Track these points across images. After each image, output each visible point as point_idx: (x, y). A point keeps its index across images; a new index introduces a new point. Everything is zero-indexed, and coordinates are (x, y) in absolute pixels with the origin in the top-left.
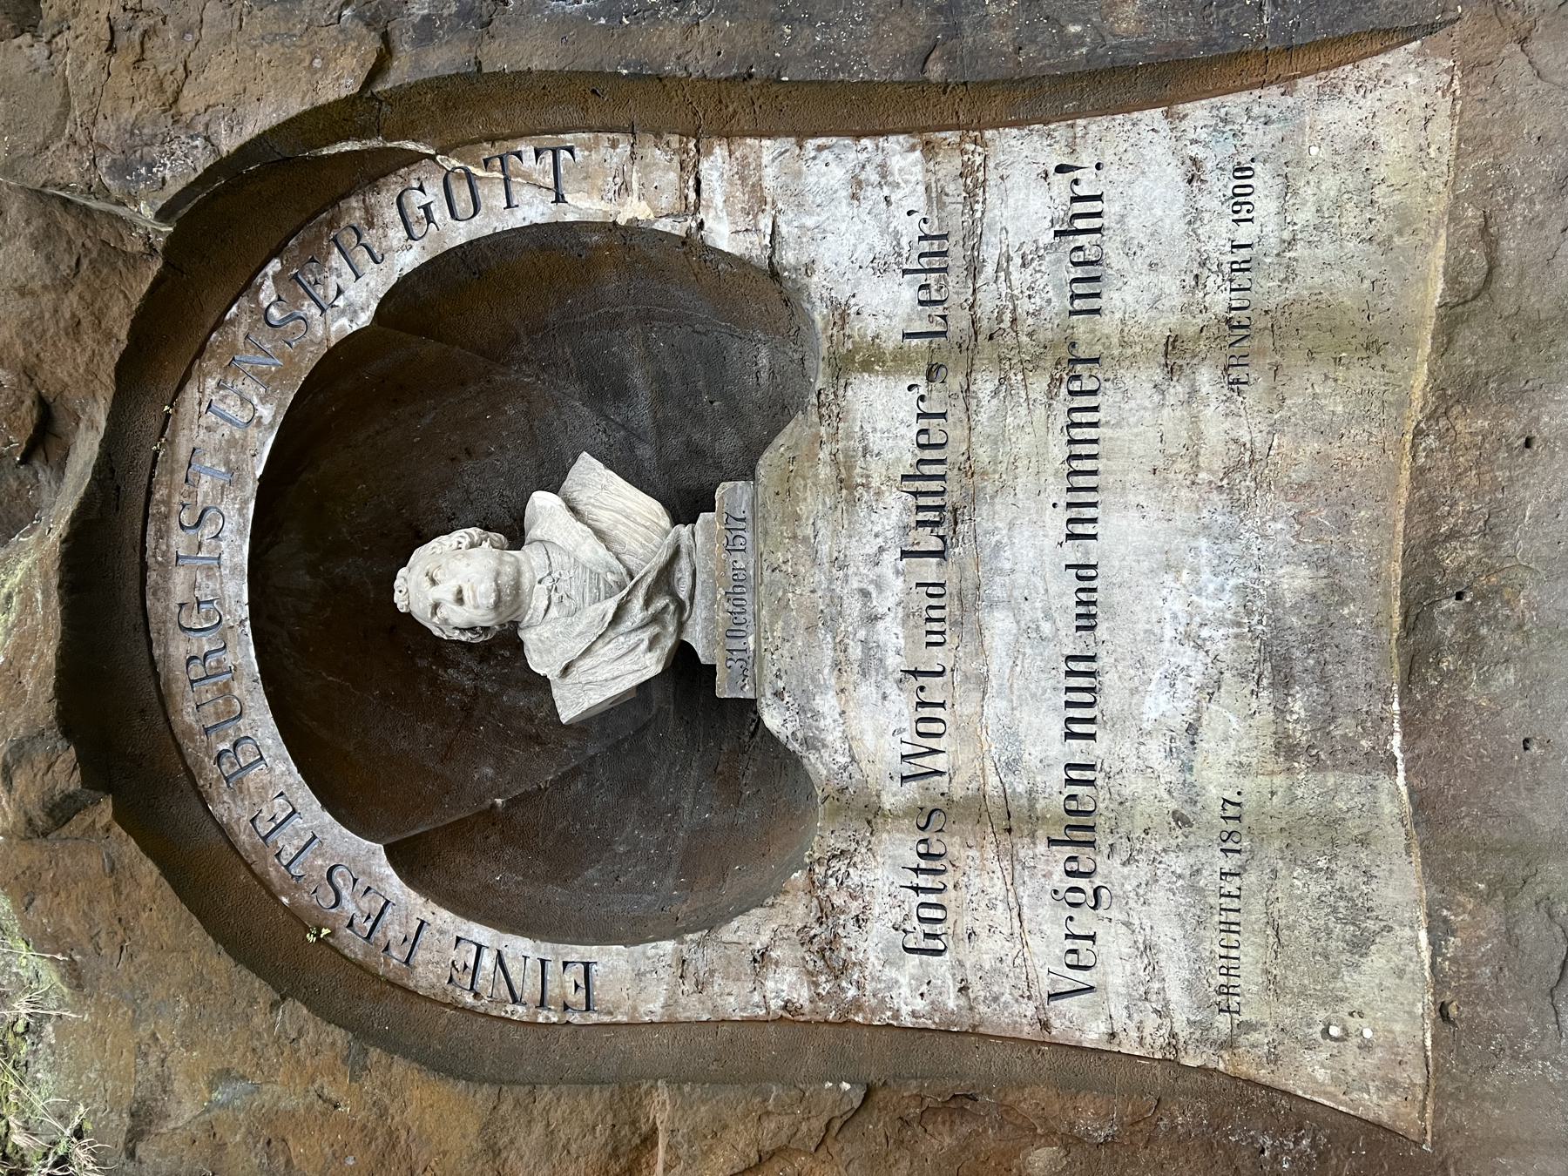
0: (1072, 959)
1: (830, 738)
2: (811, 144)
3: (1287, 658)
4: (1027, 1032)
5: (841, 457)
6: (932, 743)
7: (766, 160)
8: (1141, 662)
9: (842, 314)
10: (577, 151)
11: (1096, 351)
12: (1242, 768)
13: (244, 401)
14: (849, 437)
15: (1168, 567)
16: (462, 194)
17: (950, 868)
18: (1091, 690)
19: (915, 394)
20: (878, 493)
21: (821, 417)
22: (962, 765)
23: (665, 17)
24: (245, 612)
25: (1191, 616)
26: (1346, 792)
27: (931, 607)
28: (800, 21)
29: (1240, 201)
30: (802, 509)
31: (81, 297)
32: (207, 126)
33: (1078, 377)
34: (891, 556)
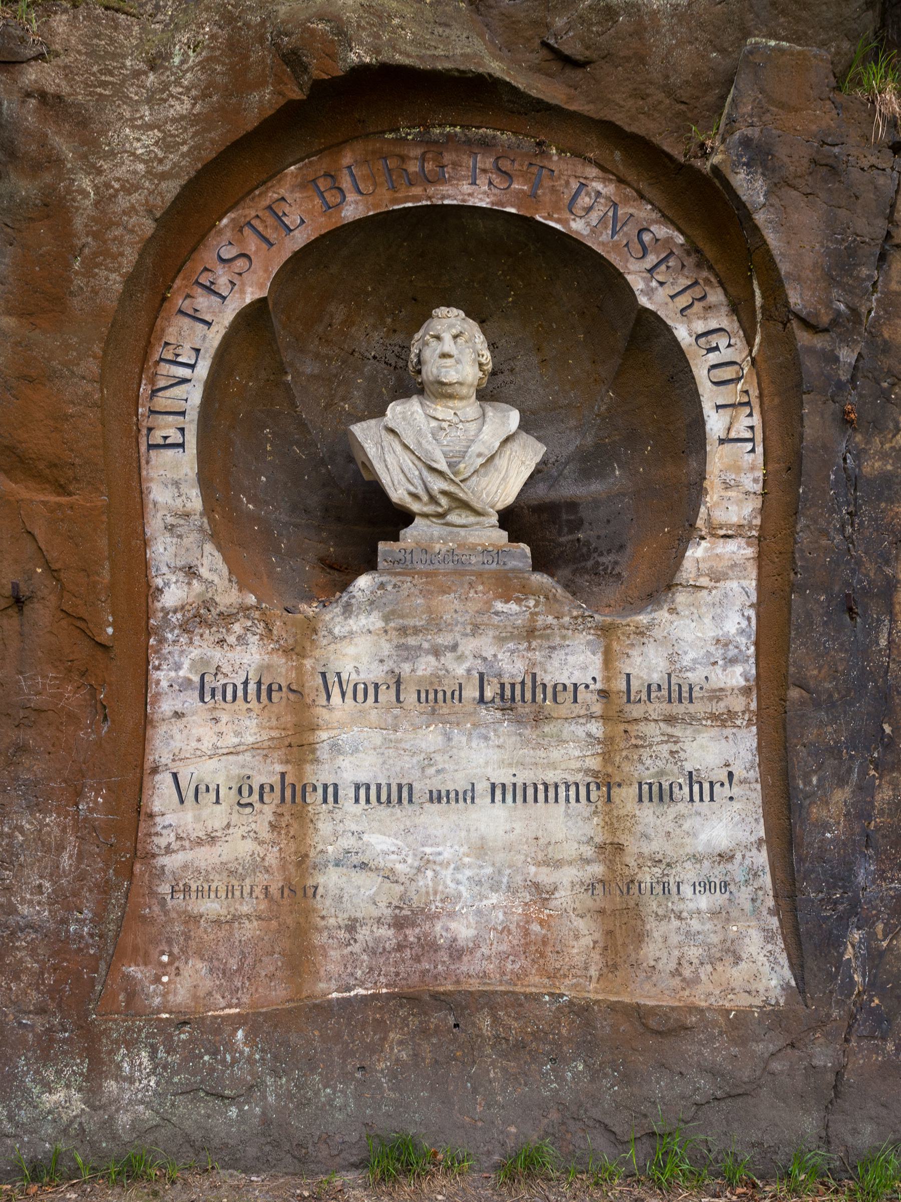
0: (202, 788)
1: (351, 622)
2: (752, 613)
3: (413, 925)
5: (549, 631)
7: (745, 583)
10: (752, 455)
11: (616, 799)
14: (564, 637)
16: (728, 373)
17: (261, 706)
18: (389, 801)
19: (590, 681)
21: (576, 618)
22: (336, 714)
23: (833, 519)
25: (441, 864)
27: (445, 692)
28: (828, 607)
29: (707, 886)
33: (598, 788)
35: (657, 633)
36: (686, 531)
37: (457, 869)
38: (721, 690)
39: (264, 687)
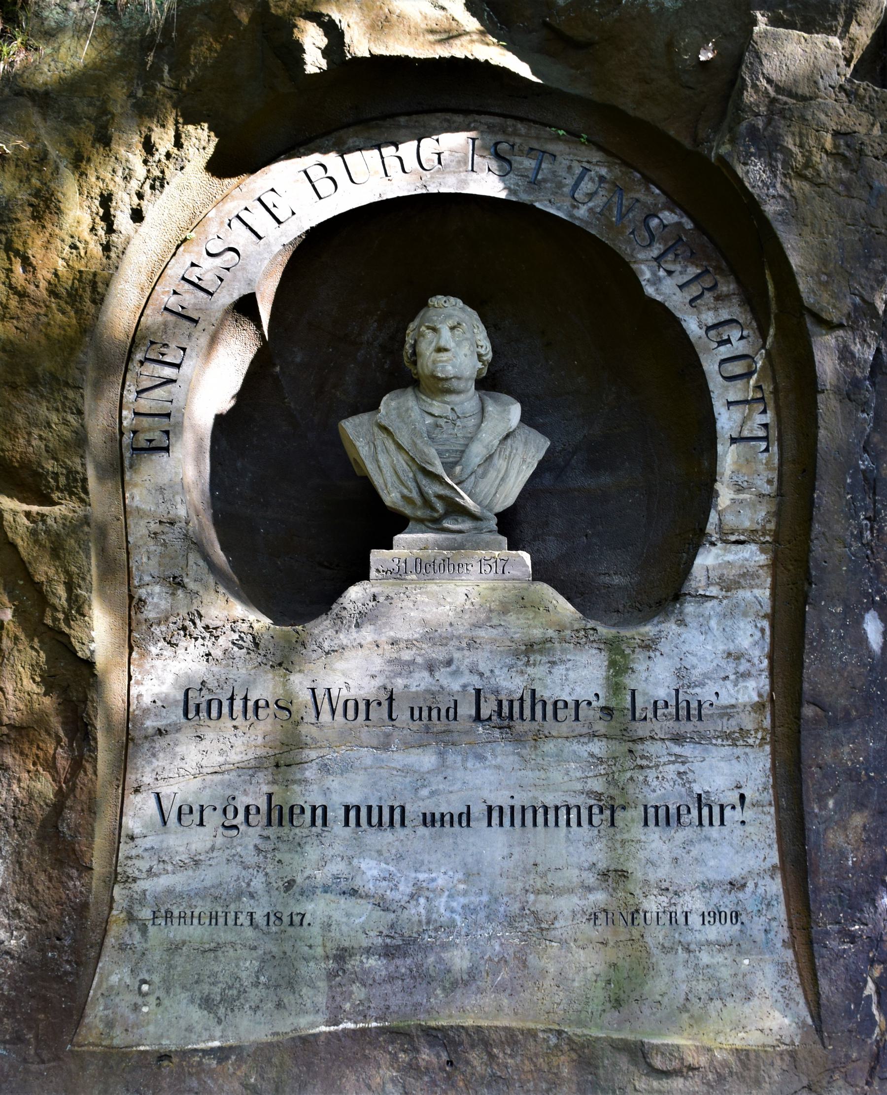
0: (186, 809)
1: (341, 636)
2: (766, 624)
3: (405, 955)
4: (131, 777)
5: (548, 645)
7: (757, 592)
8: (400, 857)
9: (649, 646)
10: (766, 454)
12: (327, 926)
13: (591, 196)
14: (564, 651)
15: (468, 875)
16: (737, 368)
17: (248, 723)
18: (380, 823)
19: (592, 698)
20: (522, 672)
21: (578, 631)
23: (850, 525)
25: (434, 891)
27: (439, 710)
28: (845, 619)
29: (717, 915)
33: (601, 812)
35: (664, 646)
36: (695, 538)
37: (451, 896)
38: (733, 706)
39: (250, 704)
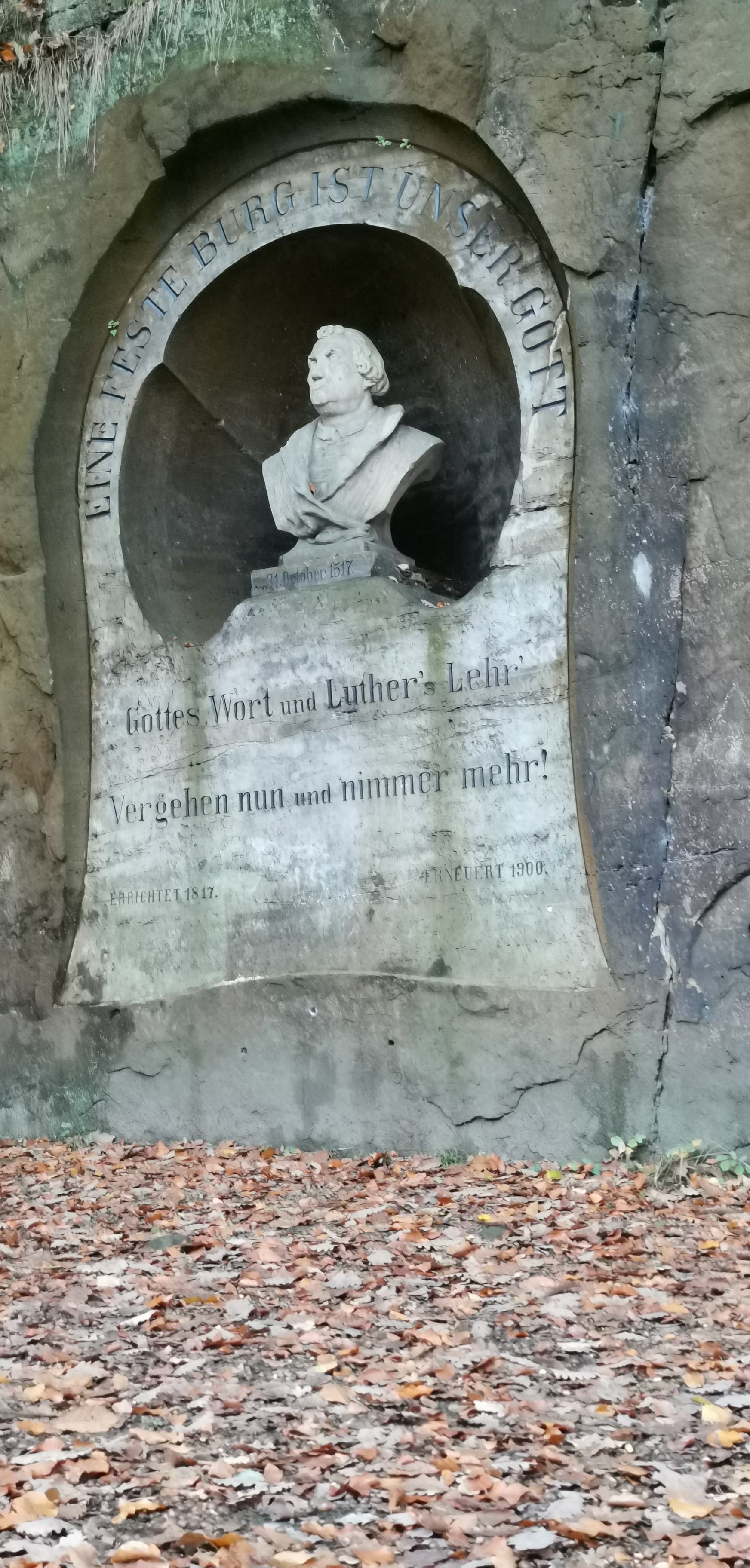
0: (131, 809)
3: (283, 917)
4: (95, 787)
5: (380, 632)
6: (232, 713)
8: (280, 834)
9: (461, 621)
11: (443, 787)
12: (228, 897)
13: (413, 199)
14: (392, 636)
15: (330, 845)
16: (539, 336)
19: (417, 675)
20: (361, 660)
22: (222, 730)
24: (287, 232)
26: (217, 954)
29: (524, 866)
30: (350, 611)
31: (450, 73)
32: (532, 157)
34: (327, 673)
35: (474, 619)
37: (318, 865)
38: (535, 667)
39: (171, 715)
